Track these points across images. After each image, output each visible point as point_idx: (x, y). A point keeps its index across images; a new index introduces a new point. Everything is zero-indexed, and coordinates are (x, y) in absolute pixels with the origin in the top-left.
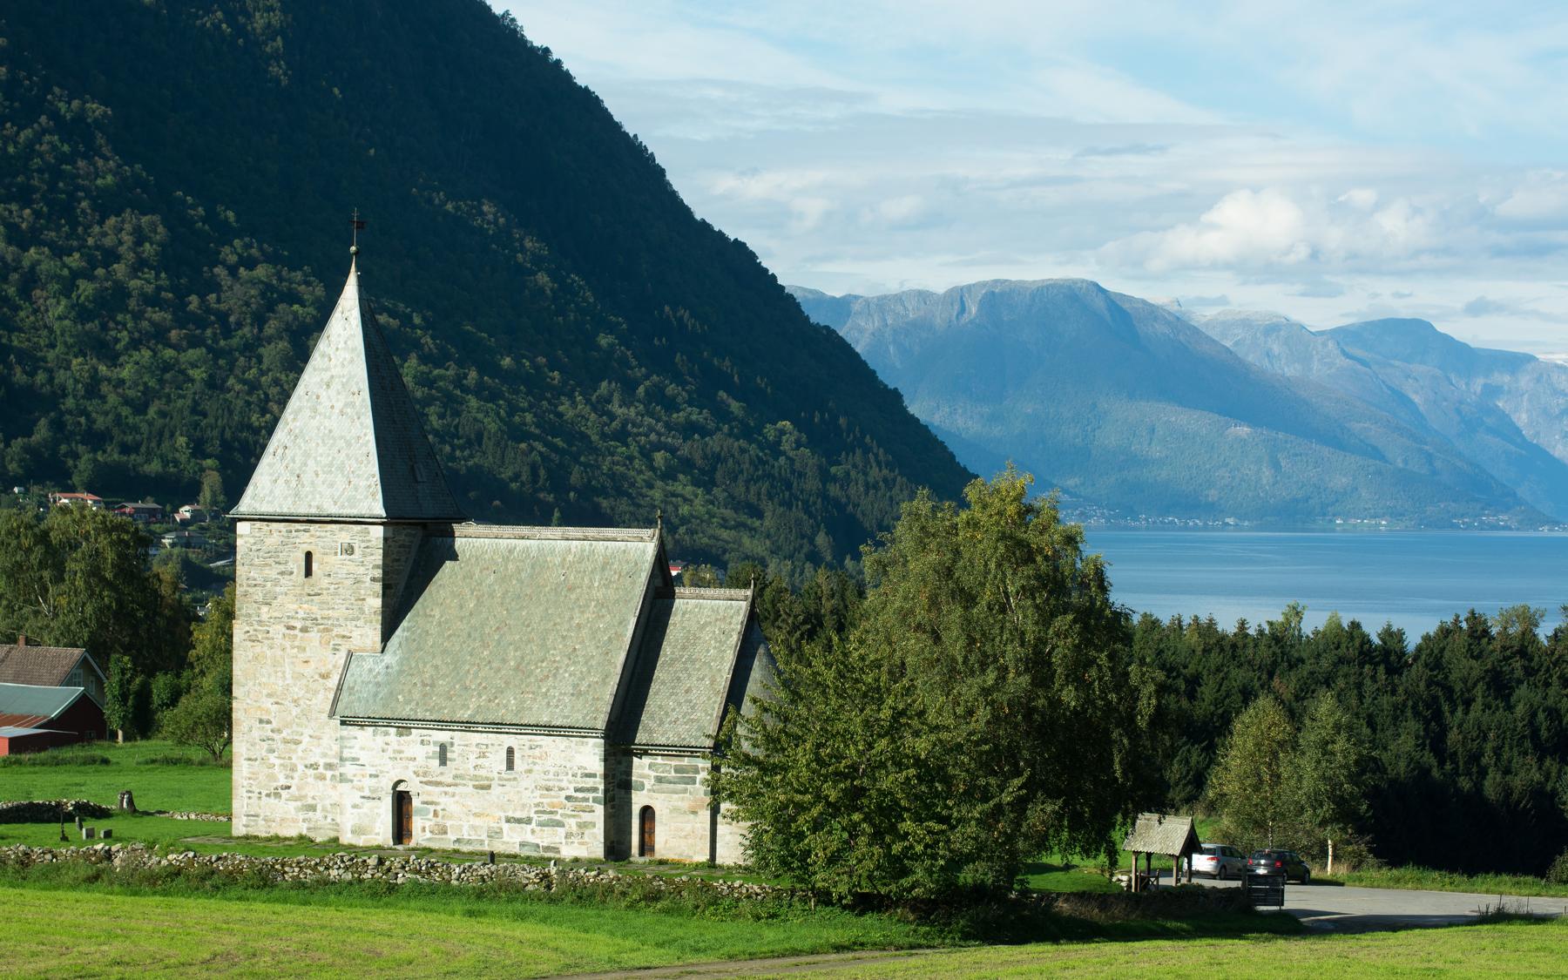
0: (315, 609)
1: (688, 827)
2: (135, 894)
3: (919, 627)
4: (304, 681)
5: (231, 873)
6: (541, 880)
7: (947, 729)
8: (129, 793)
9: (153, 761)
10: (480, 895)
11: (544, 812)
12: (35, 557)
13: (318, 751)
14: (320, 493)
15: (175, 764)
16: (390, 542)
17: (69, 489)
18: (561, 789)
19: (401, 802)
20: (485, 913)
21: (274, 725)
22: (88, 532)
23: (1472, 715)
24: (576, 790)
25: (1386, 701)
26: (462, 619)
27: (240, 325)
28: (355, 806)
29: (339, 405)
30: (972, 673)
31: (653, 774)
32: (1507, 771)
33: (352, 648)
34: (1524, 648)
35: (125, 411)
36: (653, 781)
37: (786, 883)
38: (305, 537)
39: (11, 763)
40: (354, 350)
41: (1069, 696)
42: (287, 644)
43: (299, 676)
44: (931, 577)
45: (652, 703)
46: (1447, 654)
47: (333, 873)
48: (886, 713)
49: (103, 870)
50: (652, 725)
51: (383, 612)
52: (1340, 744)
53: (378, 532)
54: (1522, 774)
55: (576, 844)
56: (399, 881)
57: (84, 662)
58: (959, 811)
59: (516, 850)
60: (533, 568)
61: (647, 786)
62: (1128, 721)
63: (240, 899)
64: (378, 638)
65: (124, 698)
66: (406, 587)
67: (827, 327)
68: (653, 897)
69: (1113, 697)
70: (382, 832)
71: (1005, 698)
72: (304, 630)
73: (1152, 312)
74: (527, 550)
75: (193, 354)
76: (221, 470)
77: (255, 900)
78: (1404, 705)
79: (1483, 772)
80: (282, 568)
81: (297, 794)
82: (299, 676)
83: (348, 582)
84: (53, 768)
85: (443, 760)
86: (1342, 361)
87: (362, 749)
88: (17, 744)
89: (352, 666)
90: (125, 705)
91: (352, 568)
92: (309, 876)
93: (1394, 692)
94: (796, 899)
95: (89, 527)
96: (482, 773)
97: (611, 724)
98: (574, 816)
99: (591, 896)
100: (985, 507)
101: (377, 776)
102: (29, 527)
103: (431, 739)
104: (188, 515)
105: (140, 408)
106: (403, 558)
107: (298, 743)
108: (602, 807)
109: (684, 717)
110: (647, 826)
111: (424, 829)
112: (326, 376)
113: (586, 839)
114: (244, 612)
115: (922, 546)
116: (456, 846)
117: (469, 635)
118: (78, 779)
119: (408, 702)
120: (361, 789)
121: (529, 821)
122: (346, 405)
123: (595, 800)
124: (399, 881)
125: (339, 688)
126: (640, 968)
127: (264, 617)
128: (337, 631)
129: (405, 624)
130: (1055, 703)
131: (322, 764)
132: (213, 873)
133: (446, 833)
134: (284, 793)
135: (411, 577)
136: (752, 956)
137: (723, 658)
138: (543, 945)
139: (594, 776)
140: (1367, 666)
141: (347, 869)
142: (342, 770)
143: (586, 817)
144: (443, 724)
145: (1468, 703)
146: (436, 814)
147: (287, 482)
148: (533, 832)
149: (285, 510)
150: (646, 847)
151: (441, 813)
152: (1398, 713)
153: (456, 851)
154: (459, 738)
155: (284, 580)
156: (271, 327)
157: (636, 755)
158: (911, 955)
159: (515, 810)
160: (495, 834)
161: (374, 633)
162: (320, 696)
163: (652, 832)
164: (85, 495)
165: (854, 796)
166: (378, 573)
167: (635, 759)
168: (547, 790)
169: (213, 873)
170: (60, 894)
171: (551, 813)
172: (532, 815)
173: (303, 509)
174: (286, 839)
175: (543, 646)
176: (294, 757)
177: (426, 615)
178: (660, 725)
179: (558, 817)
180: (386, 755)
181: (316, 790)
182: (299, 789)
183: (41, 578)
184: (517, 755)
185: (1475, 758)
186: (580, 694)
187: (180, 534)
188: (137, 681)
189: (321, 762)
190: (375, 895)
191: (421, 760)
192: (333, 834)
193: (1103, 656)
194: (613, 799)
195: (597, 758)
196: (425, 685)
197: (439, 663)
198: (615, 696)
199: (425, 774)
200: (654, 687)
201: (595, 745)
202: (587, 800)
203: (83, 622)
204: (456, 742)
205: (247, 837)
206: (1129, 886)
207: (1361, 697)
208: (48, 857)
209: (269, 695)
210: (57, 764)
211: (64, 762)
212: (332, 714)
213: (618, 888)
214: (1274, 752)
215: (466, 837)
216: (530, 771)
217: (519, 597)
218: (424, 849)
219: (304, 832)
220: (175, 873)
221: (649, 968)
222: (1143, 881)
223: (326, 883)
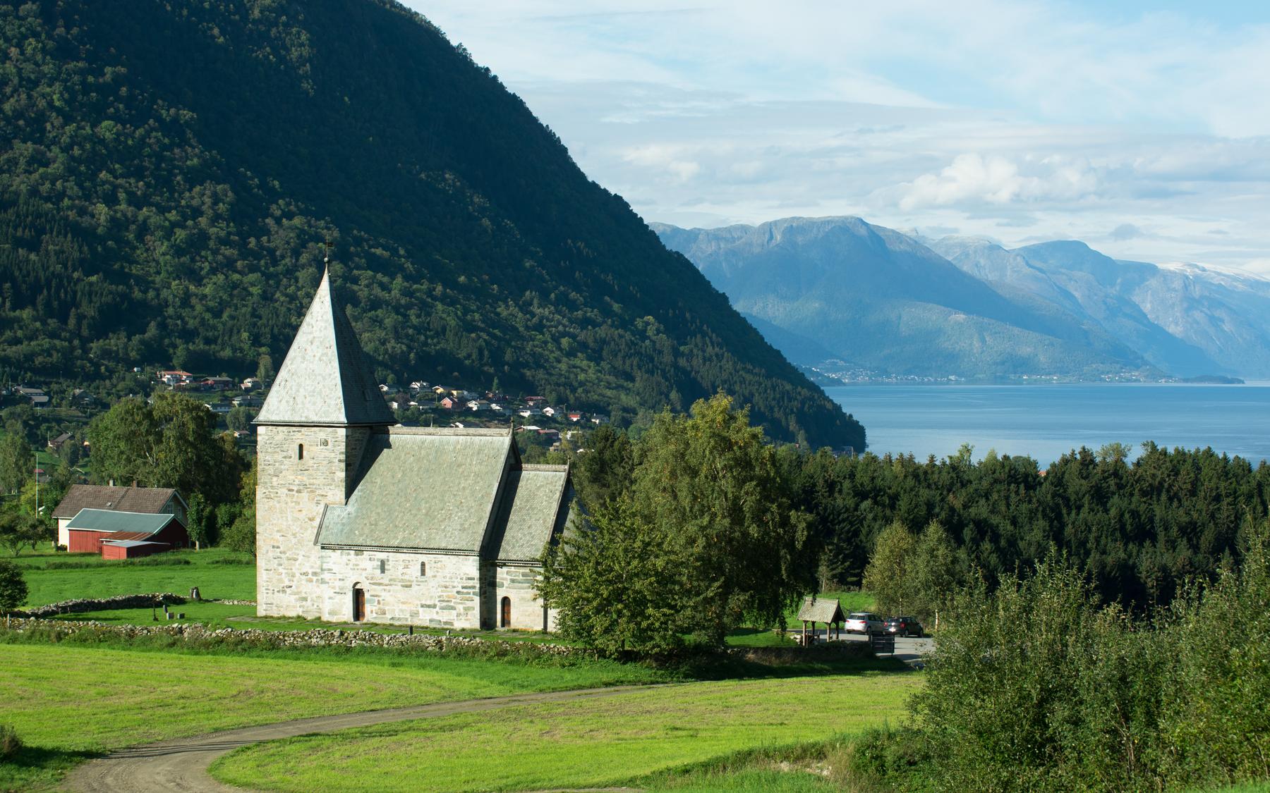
0: (305, 479)
1: (530, 609)
2: (196, 654)
3: (665, 490)
4: (299, 523)
5: (253, 641)
6: (437, 644)
7: (675, 553)
8: (196, 588)
9: (217, 562)
10: (400, 653)
11: (443, 601)
12: (143, 429)
13: (307, 564)
14: (307, 409)
15: (231, 563)
16: (349, 438)
17: (170, 368)
18: (454, 587)
19: (358, 595)
20: (402, 664)
21: (282, 549)
22: (177, 411)
23: (1081, 515)
24: (463, 588)
25: (1024, 507)
26: (394, 484)
27: (283, 257)
28: (330, 598)
29: (318, 355)
30: (696, 518)
31: (509, 577)
32: (1104, 552)
33: (328, 502)
34: (1117, 471)
35: (208, 316)
36: (509, 582)
37: (580, 645)
38: (298, 435)
39: (128, 564)
40: (327, 321)
41: (754, 531)
42: (289, 500)
44: (671, 460)
45: (508, 535)
46: (1066, 476)
47: (314, 640)
48: (638, 544)
49: (178, 639)
50: (509, 548)
51: (346, 481)
52: (941, 551)
53: (342, 432)
54: (1113, 554)
55: (463, 621)
56: (353, 645)
57: (174, 498)
58: (681, 602)
59: (427, 624)
60: (436, 452)
61: (506, 583)
62: (790, 545)
63: (258, 657)
64: (343, 496)
65: (199, 521)
66: (360, 465)
67: (677, 253)
68: (502, 654)
69: (781, 531)
70: (347, 614)
71: (715, 532)
72: (299, 491)
73: (898, 236)
74: (432, 442)
75: (252, 277)
77: (267, 657)
78: (1037, 510)
79: (1087, 553)
80: (285, 454)
81: (296, 590)
83: (325, 462)
84: (155, 567)
85: (383, 570)
87: (334, 563)
88: (132, 552)
89: (328, 513)
90: (200, 525)
91: (327, 454)
92: (299, 641)
93: (1030, 502)
94: (587, 654)
95: (178, 408)
96: (406, 577)
97: (482, 548)
98: (462, 603)
99: (466, 653)
100: (704, 416)
101: (343, 580)
102: (140, 408)
103: (376, 558)
104: (250, 385)
105: (217, 314)
106: (358, 448)
107: (296, 560)
108: (478, 598)
109: (527, 543)
110: (506, 609)
111: (372, 612)
112: (310, 337)
113: (469, 617)
114: (262, 480)
115: (666, 440)
116: (391, 622)
117: (398, 494)
118: (170, 574)
119: (361, 535)
120: (334, 588)
121: (435, 606)
122: (323, 355)
123: (474, 594)
124: (353, 645)
125: (320, 527)
126: (485, 698)
127: (275, 484)
128: (320, 492)
129: (359, 487)
130: (745, 534)
131: (310, 573)
132: (242, 641)
133: (385, 614)
134: (288, 590)
135: (363, 458)
136: (554, 690)
137: (550, 507)
138: (433, 684)
139: (474, 579)
140: (1013, 485)
141: (322, 638)
142: (322, 576)
144: (382, 548)
145: (1079, 508)
146: (379, 602)
147: (287, 402)
148: (437, 613)
149: (287, 419)
150: (505, 622)
151: (382, 602)
152: (1032, 516)
153: (391, 625)
154: (392, 557)
155: (286, 461)
156: (304, 259)
157: (499, 566)
158: (650, 688)
159: (426, 600)
160: (414, 614)
161: (340, 493)
162: (309, 532)
163: (509, 612)
164: (181, 373)
165: (618, 596)
166: (343, 457)
167: (498, 569)
168: (446, 587)
169: (242, 641)
170: (152, 654)
171: (448, 601)
172: (437, 603)
174: (290, 618)
175: (442, 501)
176: (293, 568)
177: (372, 482)
178: (512, 548)
179: (452, 604)
180: (349, 567)
182: (297, 587)
183: (148, 441)
184: (427, 567)
185: (1083, 543)
186: (464, 529)
187: (245, 397)
188: (208, 510)
189: (310, 571)
190: (338, 654)
191: (370, 570)
192: (318, 615)
193: (774, 506)
194: (485, 593)
195: (475, 568)
196: (371, 525)
197: (380, 511)
198: (486, 531)
199: (372, 578)
200: (509, 525)
201: (474, 561)
202: (469, 593)
203: (175, 469)
204: (391, 559)
205: (266, 617)
206: (801, 642)
207: (1008, 505)
208: (145, 632)
209: (278, 531)
210: (157, 565)
211: (162, 563)
212: (316, 543)
213: (482, 649)
214: (899, 557)
215: (397, 616)
216: (435, 576)
217: (428, 471)
218: (372, 624)
219: (301, 614)
220: (220, 641)
221: (491, 698)
222: (810, 639)
223: (309, 646)
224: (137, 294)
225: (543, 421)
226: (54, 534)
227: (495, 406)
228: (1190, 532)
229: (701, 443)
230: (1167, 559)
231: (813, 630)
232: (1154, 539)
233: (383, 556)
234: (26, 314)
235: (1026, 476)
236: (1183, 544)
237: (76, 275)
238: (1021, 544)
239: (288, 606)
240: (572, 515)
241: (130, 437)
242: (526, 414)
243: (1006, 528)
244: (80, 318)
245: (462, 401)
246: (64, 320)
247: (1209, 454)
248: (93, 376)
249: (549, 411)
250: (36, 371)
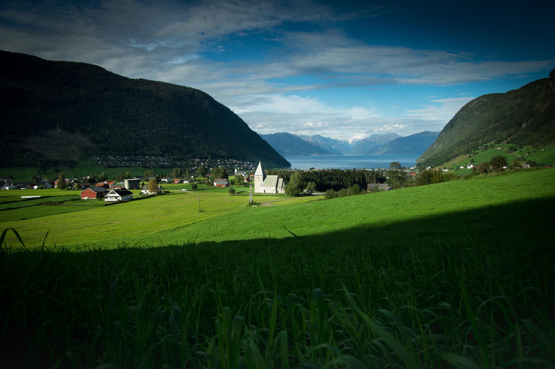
17: (197, 159)
19: (265, 190)
27: (211, 142)
34: (328, 172)
35: (201, 151)
41: (301, 184)
70: (264, 192)
73: (293, 135)
75: (207, 145)
76: (210, 156)
86: (312, 139)
88: (226, 186)
105: (202, 151)
145: (323, 177)
152: (318, 178)
156: (214, 142)
173: (258, 175)
185: (324, 181)
222: (304, 193)
223: (264, 195)
224: (191, 148)
225: (247, 164)
226: (214, 184)
227: (241, 162)
228: (337, 179)
229: (296, 177)
230: (334, 182)
231: (304, 192)
232: (333, 180)
234: (176, 152)
235: (317, 173)
236: (336, 181)
237: (183, 146)
238: (317, 181)
239: (258, 192)
241: (216, 172)
242: (245, 163)
243: (315, 179)
244: (184, 152)
245: (236, 162)
246: (181, 152)
247: (339, 169)
248: (186, 160)
249: (248, 163)
250: (178, 160)
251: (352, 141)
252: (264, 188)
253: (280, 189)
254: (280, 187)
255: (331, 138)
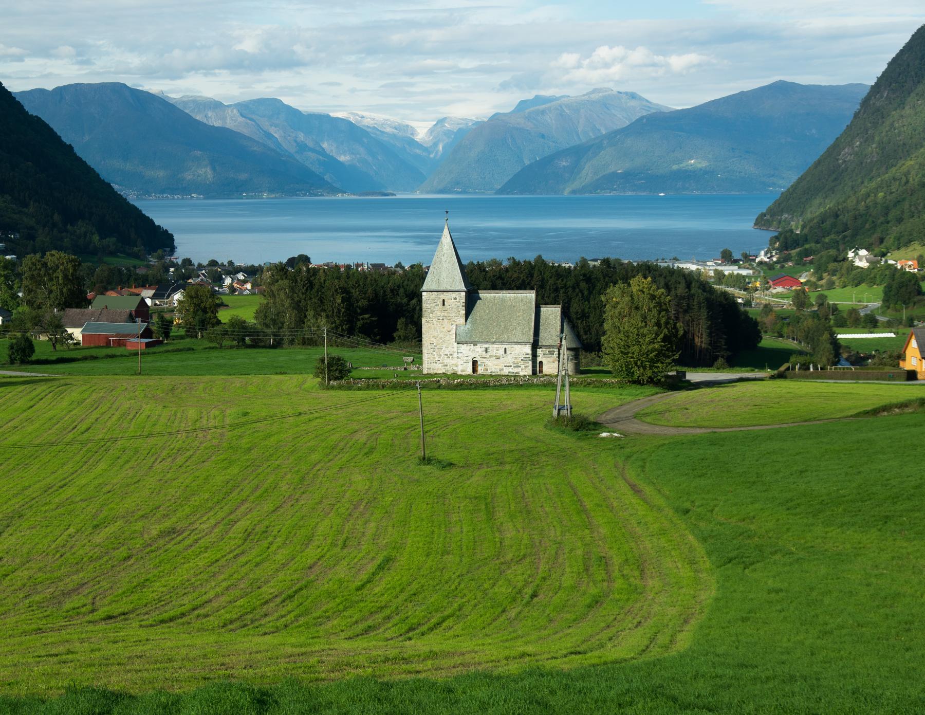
43: (441, 332)
45: (541, 335)
64: (464, 320)
67: (36, 116)
70: (469, 371)
82: (441, 332)
85: (486, 351)
86: (241, 119)
143: (527, 365)
144: (486, 343)
150: (541, 371)
154: (491, 346)
160: (501, 370)
181: (446, 361)
191: (480, 352)
233: (486, 346)
239: (439, 369)
240: (565, 326)
251: (431, 131)
252: (477, 351)
253: (551, 353)
254: (553, 347)
255: (332, 115)
